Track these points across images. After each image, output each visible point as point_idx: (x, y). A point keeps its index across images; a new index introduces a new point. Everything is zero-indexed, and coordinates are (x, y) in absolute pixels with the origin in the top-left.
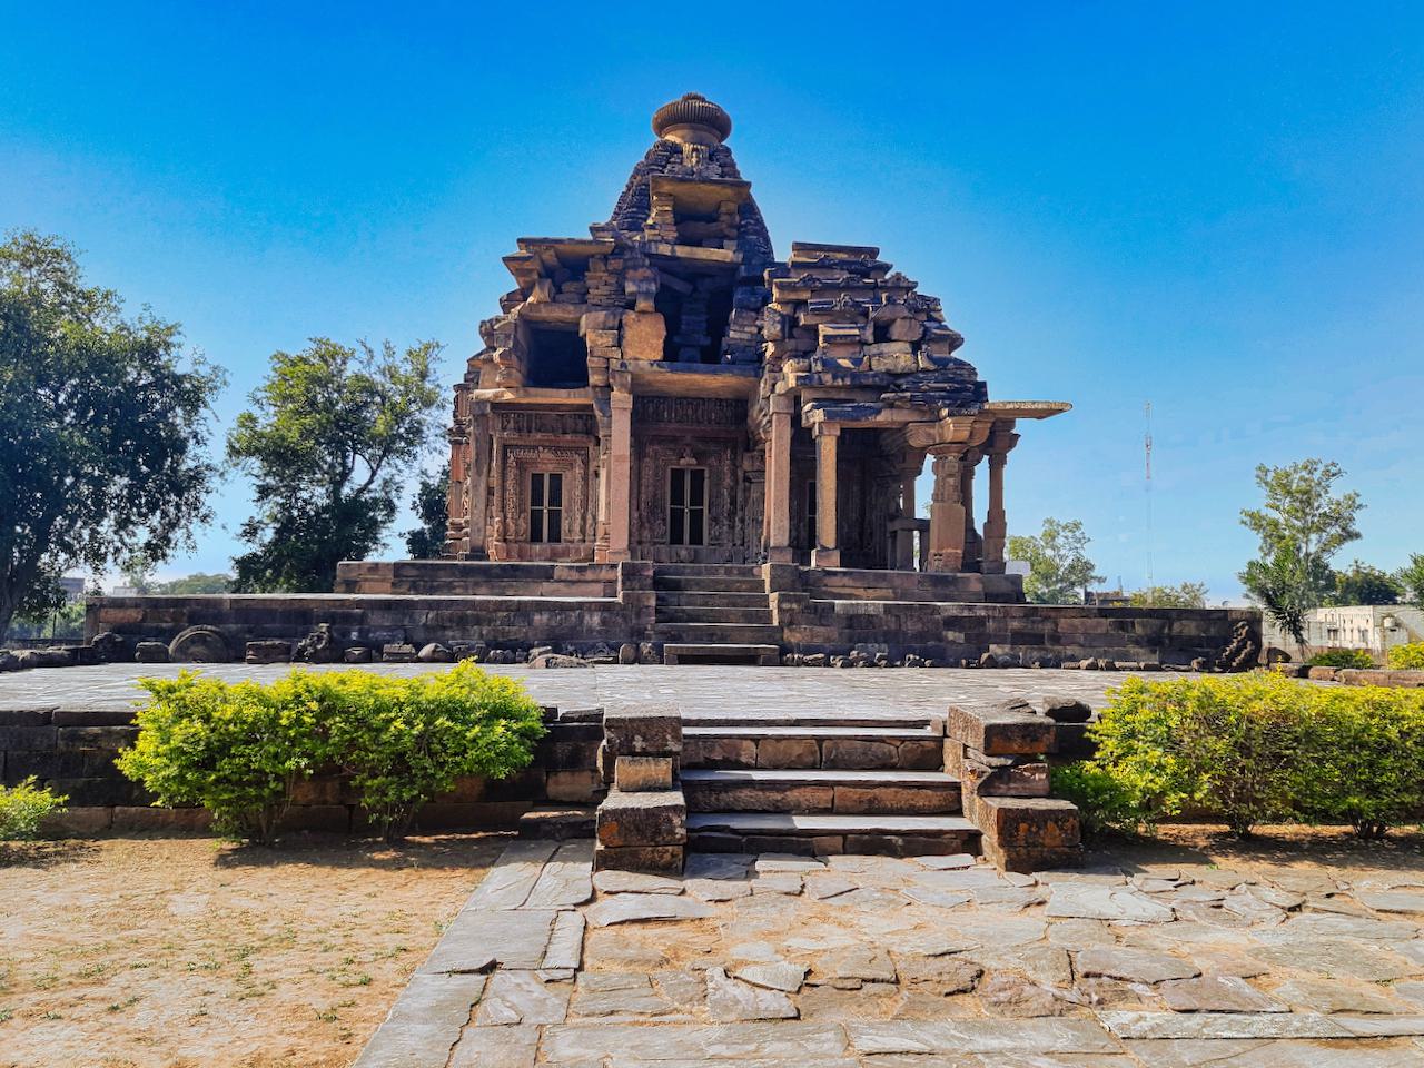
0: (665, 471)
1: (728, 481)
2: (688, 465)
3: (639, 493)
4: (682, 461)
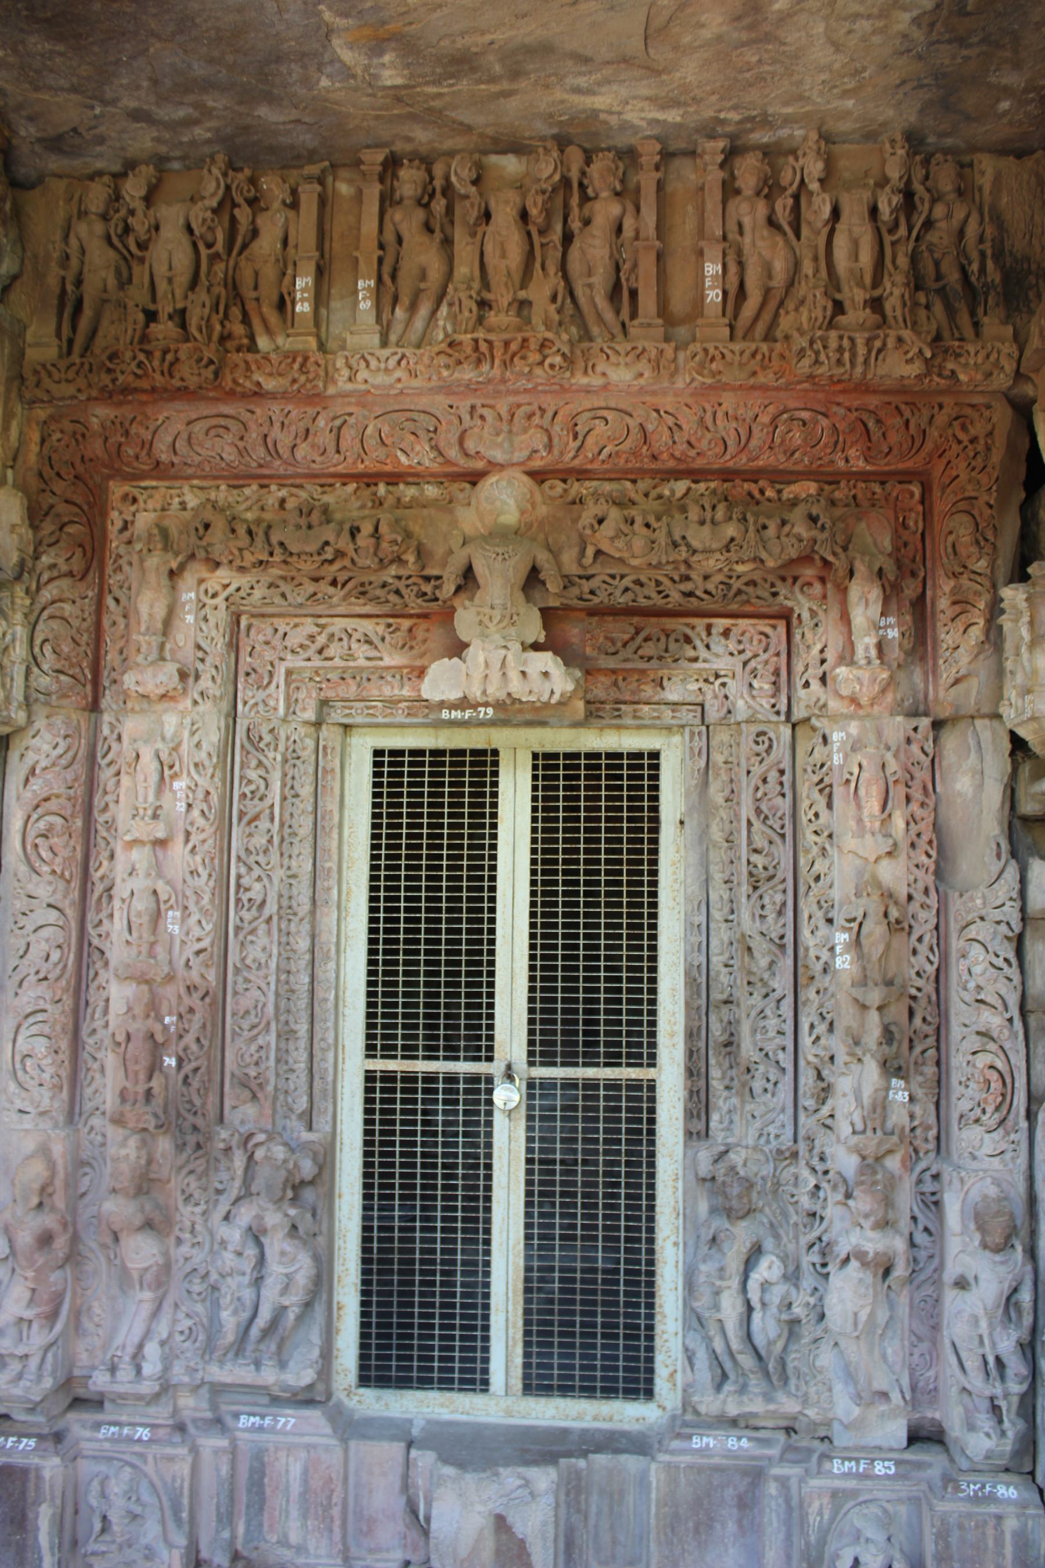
2: (510, 712)
4: (443, 681)
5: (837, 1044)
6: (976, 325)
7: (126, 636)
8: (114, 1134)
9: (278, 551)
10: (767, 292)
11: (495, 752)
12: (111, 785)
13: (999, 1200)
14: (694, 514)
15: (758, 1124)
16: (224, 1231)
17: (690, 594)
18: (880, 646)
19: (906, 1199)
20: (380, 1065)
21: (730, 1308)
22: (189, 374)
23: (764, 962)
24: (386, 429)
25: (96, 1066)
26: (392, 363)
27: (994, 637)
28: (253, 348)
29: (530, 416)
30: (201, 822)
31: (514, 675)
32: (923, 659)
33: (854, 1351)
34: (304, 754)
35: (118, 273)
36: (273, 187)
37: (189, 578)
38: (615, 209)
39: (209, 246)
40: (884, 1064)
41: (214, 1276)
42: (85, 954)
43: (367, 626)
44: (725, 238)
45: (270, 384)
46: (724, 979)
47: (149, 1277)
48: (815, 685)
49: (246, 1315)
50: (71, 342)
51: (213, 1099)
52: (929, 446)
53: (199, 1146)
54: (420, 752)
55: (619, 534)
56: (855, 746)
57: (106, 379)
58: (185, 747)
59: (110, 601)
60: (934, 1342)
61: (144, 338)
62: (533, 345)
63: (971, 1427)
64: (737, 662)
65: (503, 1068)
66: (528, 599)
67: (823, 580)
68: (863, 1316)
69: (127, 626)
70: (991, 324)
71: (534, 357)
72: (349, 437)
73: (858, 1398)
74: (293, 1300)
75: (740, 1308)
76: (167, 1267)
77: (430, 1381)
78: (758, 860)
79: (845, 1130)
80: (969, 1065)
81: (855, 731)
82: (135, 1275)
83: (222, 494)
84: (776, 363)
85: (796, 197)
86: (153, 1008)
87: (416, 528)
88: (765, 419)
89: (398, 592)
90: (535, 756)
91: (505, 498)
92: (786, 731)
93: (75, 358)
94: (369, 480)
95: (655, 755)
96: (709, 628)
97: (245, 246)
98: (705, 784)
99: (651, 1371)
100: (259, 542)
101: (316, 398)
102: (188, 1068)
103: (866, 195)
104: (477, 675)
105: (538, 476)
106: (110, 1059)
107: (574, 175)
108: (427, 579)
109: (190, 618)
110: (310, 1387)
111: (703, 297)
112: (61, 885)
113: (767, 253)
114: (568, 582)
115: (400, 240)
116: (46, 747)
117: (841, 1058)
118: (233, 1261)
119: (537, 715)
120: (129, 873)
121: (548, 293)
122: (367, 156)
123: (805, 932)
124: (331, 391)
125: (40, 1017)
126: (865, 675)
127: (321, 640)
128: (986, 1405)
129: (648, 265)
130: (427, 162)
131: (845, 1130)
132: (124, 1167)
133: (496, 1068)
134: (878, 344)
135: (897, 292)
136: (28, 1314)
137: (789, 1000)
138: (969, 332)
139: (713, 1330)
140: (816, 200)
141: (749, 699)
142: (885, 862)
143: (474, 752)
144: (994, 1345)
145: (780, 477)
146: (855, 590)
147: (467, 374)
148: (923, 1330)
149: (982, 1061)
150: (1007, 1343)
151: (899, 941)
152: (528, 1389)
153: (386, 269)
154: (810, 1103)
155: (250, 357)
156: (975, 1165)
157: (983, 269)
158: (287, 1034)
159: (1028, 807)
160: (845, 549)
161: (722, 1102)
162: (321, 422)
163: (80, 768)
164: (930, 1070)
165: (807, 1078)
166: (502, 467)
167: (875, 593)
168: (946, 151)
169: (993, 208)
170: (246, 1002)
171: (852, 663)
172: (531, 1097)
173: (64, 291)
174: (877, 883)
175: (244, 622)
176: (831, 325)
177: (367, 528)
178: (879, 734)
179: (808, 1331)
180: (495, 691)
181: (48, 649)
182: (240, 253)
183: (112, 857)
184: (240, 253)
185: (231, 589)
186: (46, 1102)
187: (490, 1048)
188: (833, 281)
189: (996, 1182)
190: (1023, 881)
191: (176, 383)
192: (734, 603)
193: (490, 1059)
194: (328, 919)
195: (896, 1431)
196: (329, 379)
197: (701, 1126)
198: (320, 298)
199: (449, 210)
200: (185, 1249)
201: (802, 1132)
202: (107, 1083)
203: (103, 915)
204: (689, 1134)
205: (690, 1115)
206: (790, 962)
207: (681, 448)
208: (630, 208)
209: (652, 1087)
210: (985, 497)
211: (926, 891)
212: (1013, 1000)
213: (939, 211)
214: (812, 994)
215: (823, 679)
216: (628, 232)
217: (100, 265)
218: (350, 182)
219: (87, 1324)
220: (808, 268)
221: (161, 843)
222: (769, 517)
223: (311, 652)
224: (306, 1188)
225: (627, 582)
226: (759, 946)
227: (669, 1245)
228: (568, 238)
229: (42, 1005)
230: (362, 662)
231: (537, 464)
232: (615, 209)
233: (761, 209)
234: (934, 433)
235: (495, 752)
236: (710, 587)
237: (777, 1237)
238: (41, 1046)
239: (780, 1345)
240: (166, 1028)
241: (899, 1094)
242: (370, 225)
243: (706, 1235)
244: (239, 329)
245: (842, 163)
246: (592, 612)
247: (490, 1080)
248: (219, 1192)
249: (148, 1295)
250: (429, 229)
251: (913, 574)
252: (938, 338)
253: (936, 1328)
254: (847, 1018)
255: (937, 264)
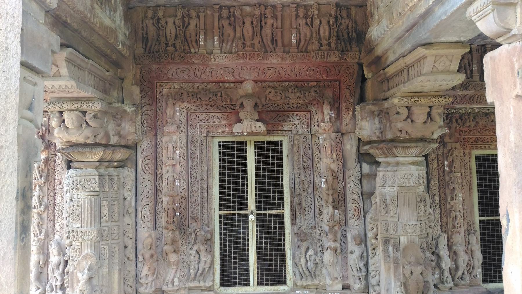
0: (208, 149)
1: (326, 161)
2: (250, 134)
3: (157, 191)
4: (237, 128)
5: (323, 203)
6: (351, 46)
7: (163, 118)
8: (165, 231)
9: (199, 99)
10: (305, 40)
11: (246, 142)
12: (161, 153)
13: (358, 234)
14: (290, 91)
15: (307, 221)
16: (191, 252)
17: (289, 107)
18: (330, 118)
19: (339, 236)
20: (222, 212)
21: (303, 261)
22: (177, 59)
23: (307, 186)
24: (222, 72)
25: (160, 216)
26: (224, 57)
27: (354, 116)
28: (191, 53)
29: (254, 69)
30: (183, 160)
31: (253, 127)
32: (339, 119)
33: (329, 268)
34: (204, 144)
35: (156, 32)
36: (193, 13)
37: (177, 105)
38: (272, 21)
39: (179, 27)
40: (333, 207)
41: (189, 262)
42: (157, 191)
43: (218, 115)
44: (296, 28)
45: (196, 62)
46: (298, 190)
47: (175, 263)
48: (316, 127)
49: (196, 271)
50: (145, 49)
51: (187, 222)
52: (340, 74)
53: (185, 233)
54: (229, 142)
55: (274, 96)
56: (325, 140)
57: (157, 60)
58: (178, 143)
59: (158, 110)
60: (347, 266)
61: (166, 50)
62: (256, 55)
63: (355, 283)
64: (299, 121)
65: (251, 211)
66: (255, 110)
67: (318, 104)
68: (331, 261)
69: (163, 115)
70: (355, 48)
71: (256, 58)
72: (214, 74)
73: (331, 279)
74: (207, 266)
75: (305, 261)
76: (179, 261)
77: (236, 284)
78: (305, 164)
79: (325, 221)
80: (351, 206)
81: (325, 135)
82: (172, 263)
83: (184, 85)
84: (307, 58)
85: (312, 18)
86: (174, 203)
87: (229, 94)
88: (305, 69)
89: (225, 108)
90: (255, 142)
91: (248, 87)
92: (310, 136)
93: (147, 52)
94: (218, 82)
95: (281, 141)
96: (293, 114)
97: (187, 27)
98: (293, 147)
99: (286, 278)
100: (194, 95)
101: (208, 65)
102: (182, 215)
103: (327, 19)
104: (245, 127)
105: (256, 82)
106: (164, 215)
107: (263, 12)
108: (232, 105)
109: (178, 114)
110: (210, 286)
111: (292, 42)
112: (151, 175)
113: (305, 31)
114: (263, 105)
115: (223, 27)
116: (146, 144)
117: (324, 206)
118: (193, 258)
119: (257, 134)
120: (166, 171)
121: (258, 42)
122: (215, 6)
123: (316, 179)
124: (210, 63)
125: (147, 206)
126: (327, 125)
127: (207, 118)
128: (357, 278)
129: (279, 34)
130: (229, 8)
131: (325, 221)
132: (169, 238)
133: (249, 212)
134: (329, 54)
135: (334, 41)
136: (148, 274)
137: (312, 194)
138: (349, 49)
139: (299, 267)
140: (316, 20)
141: (302, 129)
142: (332, 164)
143: (241, 142)
144: (359, 265)
145: (308, 81)
146: (325, 106)
147: (241, 61)
148: (344, 264)
149: (354, 205)
150: (361, 265)
151: (335, 180)
152: (258, 285)
153: (221, 34)
154: (318, 216)
155: (191, 55)
156: (353, 227)
157: (352, 34)
158: (202, 206)
159: (362, 152)
160: (322, 97)
161: (299, 217)
162: (208, 70)
163: (153, 149)
164: (343, 208)
165: (317, 211)
166: (248, 80)
167: (329, 107)
168: (345, 6)
169: (355, 20)
170: (193, 200)
171: (324, 122)
172: (257, 218)
173: (143, 37)
174: (330, 168)
175: (189, 114)
176: (319, 50)
177: (219, 94)
178: (330, 137)
179: (320, 266)
180: (249, 130)
181: (145, 122)
182: (186, 28)
183: (162, 169)
184: (186, 28)
185: (187, 107)
186: (150, 225)
187: (247, 207)
188: (320, 39)
189: (358, 231)
190: (361, 167)
191: (175, 61)
192: (299, 108)
193: (247, 210)
194: (211, 180)
195: (340, 286)
196: (210, 60)
197: (295, 222)
198: (205, 40)
199: (235, 20)
200: (182, 256)
201: (316, 222)
202: (163, 220)
203: (160, 182)
204: (292, 224)
205: (292, 220)
206: (312, 185)
207: (287, 76)
208: (275, 20)
209: (283, 214)
210: (352, 86)
211: (341, 170)
212: (360, 192)
213: (343, 21)
214: (317, 193)
215: (318, 125)
216: (275, 26)
217: (152, 30)
218: (210, 11)
219: (159, 276)
220: (314, 35)
221: (174, 165)
222: (306, 91)
223: (205, 121)
224: (208, 241)
225: (275, 105)
226: (306, 183)
227: (288, 249)
228: (261, 27)
229: (148, 203)
230: (217, 123)
231: (256, 79)
232: (272, 21)
233: (304, 21)
234: (341, 72)
235: (246, 142)
236: (294, 106)
237: (312, 245)
238: (148, 213)
239: (314, 269)
240: (177, 207)
241: (337, 213)
242: (216, 24)
243: (297, 246)
244: (187, 48)
245: (322, 9)
246: (267, 111)
247: (248, 214)
248: (189, 243)
249: (175, 267)
250: (230, 24)
251: (337, 102)
252: (343, 51)
253: (347, 263)
254: (325, 197)
255: (342, 33)
